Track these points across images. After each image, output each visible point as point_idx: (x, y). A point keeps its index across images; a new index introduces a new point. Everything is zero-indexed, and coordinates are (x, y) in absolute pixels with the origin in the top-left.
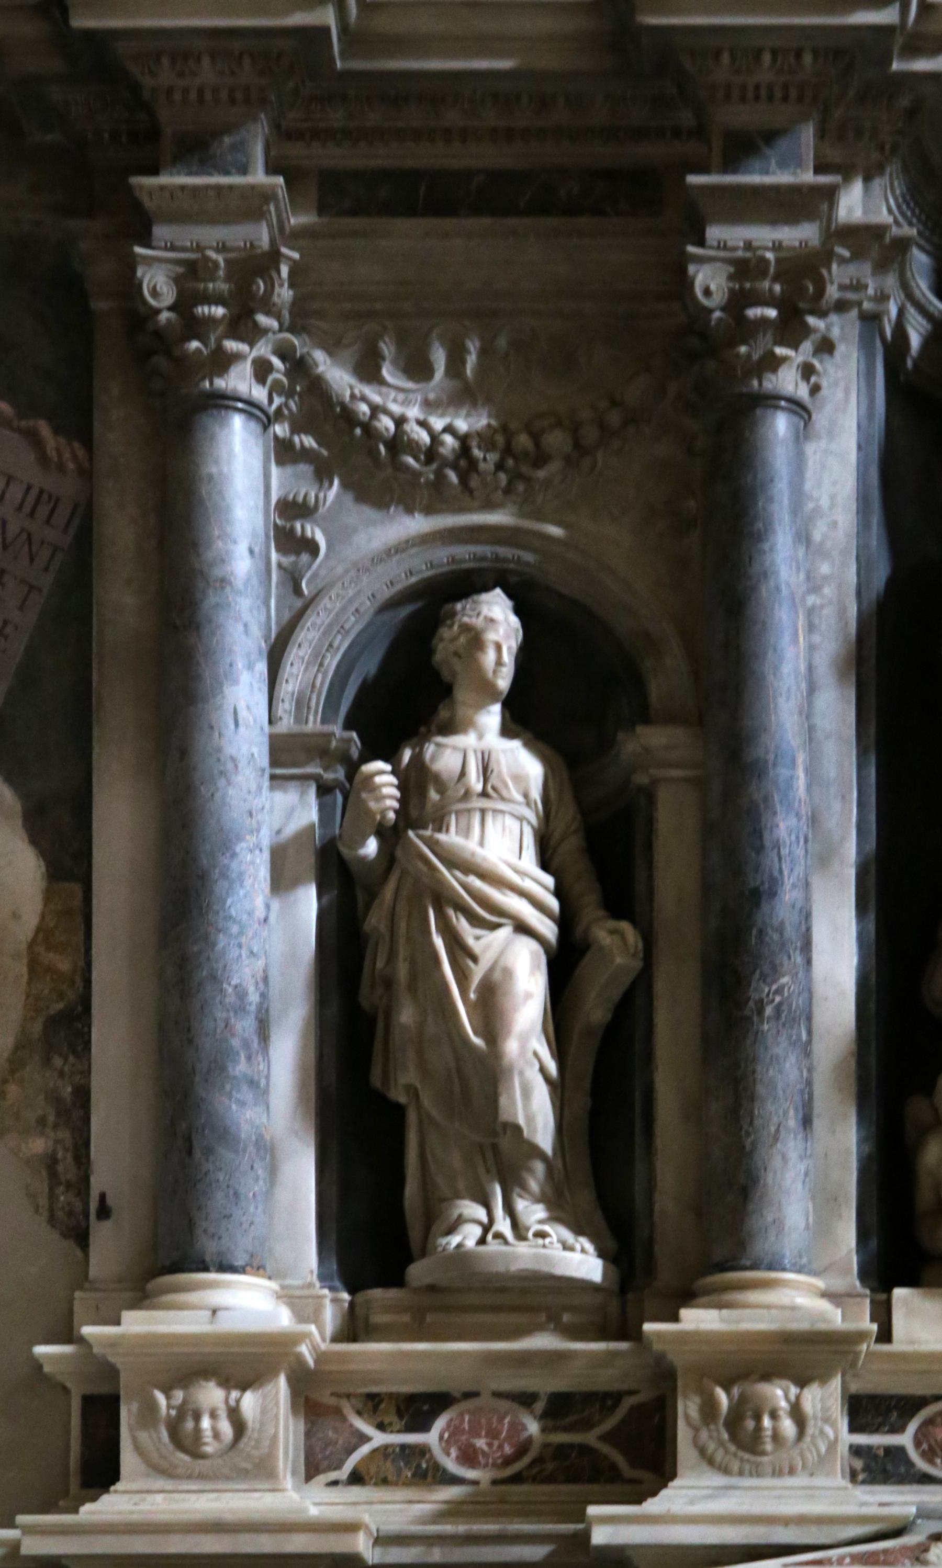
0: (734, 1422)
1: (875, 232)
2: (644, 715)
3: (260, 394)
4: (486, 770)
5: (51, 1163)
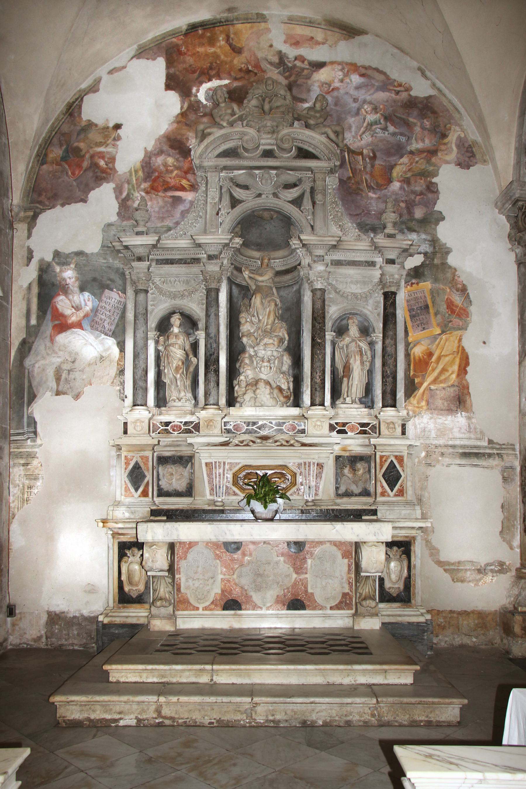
5: (120, 390)
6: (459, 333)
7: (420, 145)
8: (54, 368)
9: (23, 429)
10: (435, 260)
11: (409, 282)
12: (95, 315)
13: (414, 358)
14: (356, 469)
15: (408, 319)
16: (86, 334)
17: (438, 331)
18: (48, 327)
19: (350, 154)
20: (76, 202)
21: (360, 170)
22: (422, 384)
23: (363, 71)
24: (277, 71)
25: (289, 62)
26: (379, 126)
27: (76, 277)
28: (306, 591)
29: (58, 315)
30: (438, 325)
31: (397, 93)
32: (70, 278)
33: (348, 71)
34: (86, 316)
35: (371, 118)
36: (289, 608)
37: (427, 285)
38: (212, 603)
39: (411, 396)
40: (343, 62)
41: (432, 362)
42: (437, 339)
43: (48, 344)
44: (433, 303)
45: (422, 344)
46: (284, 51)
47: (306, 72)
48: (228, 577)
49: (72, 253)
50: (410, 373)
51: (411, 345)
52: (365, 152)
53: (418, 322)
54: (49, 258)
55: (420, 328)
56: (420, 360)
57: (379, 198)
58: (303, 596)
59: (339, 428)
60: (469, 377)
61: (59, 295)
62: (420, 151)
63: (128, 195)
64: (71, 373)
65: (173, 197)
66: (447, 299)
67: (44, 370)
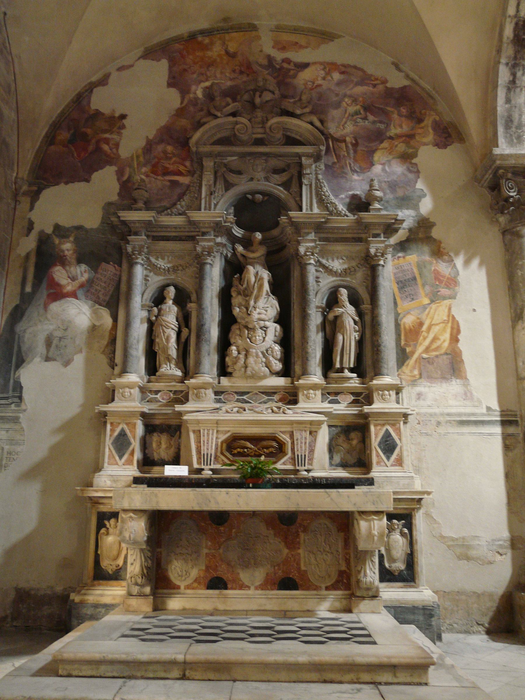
0: (196, 395)
1: (221, 243)
2: (191, 302)
3: (142, 262)
4: (169, 308)
6: (447, 302)
7: (398, 131)
8: (46, 335)
9: (8, 393)
10: (420, 234)
11: (395, 256)
12: (91, 286)
13: (405, 328)
14: (350, 438)
15: (396, 290)
16: (81, 304)
17: (426, 301)
18: (43, 293)
19: (335, 142)
20: (79, 181)
21: (344, 156)
22: (413, 353)
23: (343, 69)
24: (267, 72)
25: (277, 64)
26: (359, 116)
27: (74, 250)
28: (299, 569)
29: (54, 285)
30: (426, 295)
31: (375, 86)
32: (68, 250)
33: (329, 70)
34: (82, 286)
35: (352, 109)
36: (280, 589)
38: (196, 581)
39: (403, 364)
40: (324, 62)
41: (422, 332)
42: (426, 308)
43: (42, 311)
44: (420, 274)
45: (411, 314)
46: (272, 55)
47: (292, 72)
48: (213, 551)
49: (73, 227)
50: (401, 342)
51: (401, 316)
52: (348, 139)
53: (407, 293)
54: (49, 230)
55: (409, 299)
56: (410, 330)
57: (363, 180)
58: (295, 574)
59: (331, 398)
60: (461, 345)
61: (56, 265)
62: (399, 136)
63: (129, 177)
64: (62, 340)
65: (170, 181)
66: (434, 270)
67: (35, 336)
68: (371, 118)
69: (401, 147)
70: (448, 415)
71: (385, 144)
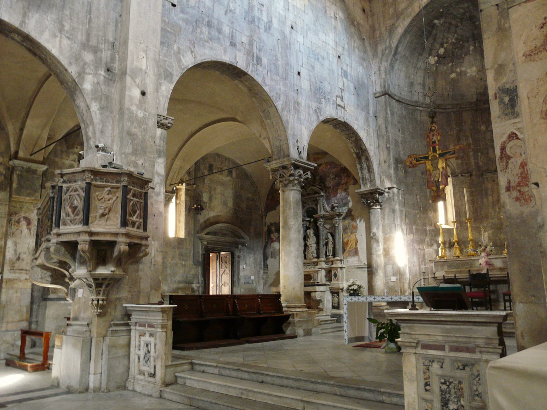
17: (350, 234)
29: (272, 239)
35: (332, 177)
37: (347, 221)
54: (269, 224)
60: (358, 246)
68: (337, 179)
69: (345, 187)
70: (355, 266)
71: (340, 187)
